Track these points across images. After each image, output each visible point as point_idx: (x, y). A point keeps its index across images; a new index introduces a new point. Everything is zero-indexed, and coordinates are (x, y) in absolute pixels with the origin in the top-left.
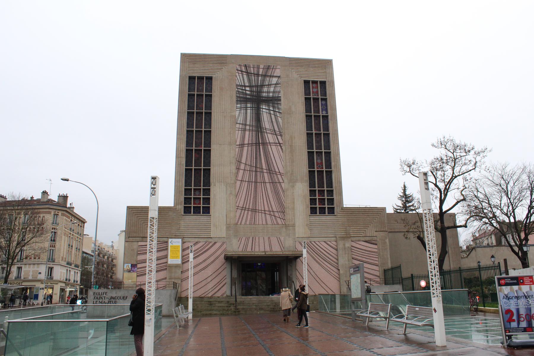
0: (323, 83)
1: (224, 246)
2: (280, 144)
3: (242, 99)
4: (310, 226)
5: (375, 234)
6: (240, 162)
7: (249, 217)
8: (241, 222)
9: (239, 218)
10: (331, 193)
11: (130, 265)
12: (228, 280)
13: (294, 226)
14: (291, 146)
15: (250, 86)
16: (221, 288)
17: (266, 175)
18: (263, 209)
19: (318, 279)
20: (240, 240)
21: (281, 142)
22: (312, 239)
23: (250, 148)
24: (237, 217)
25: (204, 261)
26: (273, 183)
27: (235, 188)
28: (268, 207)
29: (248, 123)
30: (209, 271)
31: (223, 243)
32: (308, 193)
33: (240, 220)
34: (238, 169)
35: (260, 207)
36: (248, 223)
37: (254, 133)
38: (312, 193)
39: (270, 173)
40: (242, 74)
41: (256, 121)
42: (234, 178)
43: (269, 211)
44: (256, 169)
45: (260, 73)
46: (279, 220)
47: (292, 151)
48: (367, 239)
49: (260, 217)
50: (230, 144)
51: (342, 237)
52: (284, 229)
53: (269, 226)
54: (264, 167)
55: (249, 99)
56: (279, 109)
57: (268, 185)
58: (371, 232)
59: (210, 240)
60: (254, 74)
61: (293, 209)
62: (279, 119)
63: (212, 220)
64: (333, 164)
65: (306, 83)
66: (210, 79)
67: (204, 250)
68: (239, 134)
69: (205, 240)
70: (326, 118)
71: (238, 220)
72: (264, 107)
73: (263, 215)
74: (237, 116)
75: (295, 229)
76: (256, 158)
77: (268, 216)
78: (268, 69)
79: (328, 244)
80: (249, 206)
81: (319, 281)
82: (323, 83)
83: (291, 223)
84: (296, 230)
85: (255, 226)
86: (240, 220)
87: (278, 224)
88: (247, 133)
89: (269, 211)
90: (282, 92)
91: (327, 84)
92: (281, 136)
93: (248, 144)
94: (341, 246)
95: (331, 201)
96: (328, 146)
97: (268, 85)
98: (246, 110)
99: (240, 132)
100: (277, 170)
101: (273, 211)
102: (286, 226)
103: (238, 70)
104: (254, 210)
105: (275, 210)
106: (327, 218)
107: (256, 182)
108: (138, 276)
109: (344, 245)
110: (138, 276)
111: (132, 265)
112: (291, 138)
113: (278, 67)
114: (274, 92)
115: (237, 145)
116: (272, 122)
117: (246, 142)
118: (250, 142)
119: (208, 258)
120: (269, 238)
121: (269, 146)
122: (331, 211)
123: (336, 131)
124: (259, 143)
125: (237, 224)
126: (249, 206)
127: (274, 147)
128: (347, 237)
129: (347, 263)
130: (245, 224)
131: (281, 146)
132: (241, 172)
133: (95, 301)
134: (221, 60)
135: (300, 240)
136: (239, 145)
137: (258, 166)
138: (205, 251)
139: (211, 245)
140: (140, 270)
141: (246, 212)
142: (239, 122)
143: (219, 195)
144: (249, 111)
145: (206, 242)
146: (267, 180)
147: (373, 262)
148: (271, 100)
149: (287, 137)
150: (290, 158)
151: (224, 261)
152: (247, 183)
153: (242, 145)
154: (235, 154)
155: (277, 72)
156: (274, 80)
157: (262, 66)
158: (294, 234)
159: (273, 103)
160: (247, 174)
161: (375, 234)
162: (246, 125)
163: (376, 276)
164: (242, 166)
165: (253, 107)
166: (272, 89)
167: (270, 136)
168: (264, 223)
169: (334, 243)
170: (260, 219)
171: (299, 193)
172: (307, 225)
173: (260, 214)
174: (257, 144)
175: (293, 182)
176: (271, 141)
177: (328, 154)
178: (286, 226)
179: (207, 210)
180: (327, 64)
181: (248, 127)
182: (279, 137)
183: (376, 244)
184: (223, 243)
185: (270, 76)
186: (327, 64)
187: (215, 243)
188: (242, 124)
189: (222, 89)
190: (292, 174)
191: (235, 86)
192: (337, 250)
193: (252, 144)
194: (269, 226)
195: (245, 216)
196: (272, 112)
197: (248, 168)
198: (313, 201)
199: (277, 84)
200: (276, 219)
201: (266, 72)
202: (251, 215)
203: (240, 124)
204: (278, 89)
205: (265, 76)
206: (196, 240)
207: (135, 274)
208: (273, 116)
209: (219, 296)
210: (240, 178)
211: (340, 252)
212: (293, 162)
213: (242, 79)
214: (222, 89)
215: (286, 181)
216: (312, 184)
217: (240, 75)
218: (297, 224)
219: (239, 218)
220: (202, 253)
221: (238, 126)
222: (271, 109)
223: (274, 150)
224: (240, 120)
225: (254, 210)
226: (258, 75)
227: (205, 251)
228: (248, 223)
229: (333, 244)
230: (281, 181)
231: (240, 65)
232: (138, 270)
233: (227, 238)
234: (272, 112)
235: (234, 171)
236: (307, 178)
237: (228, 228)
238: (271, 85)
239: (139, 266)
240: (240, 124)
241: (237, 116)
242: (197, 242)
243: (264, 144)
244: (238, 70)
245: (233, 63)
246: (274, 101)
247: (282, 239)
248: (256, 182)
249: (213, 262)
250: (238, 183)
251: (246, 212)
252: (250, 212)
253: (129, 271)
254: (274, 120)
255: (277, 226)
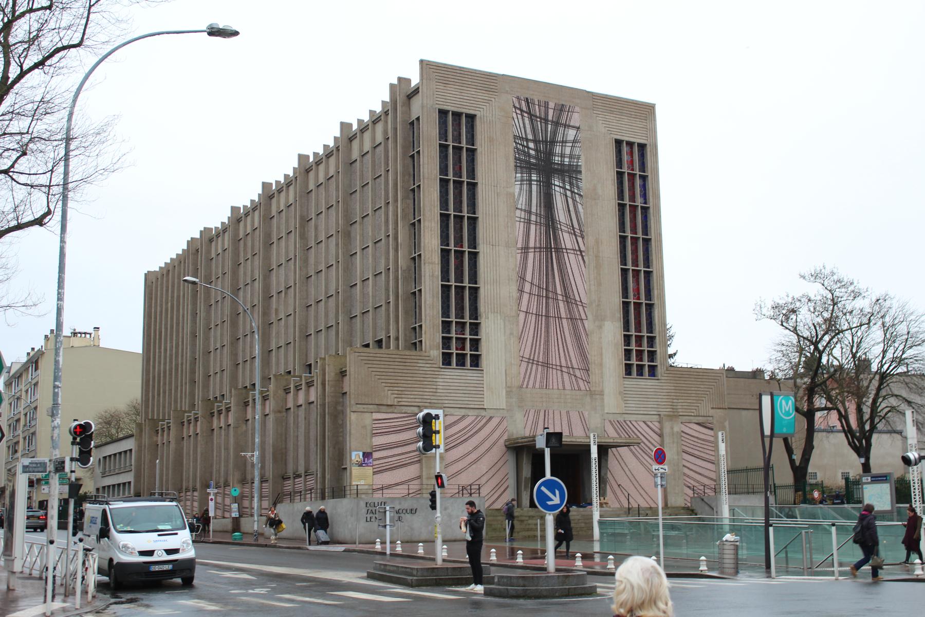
0: (642, 147)
1: (505, 423)
2: (581, 252)
3: (524, 165)
4: (624, 394)
5: (712, 412)
6: (523, 279)
7: (539, 376)
8: (528, 385)
9: (524, 378)
10: (651, 340)
11: (361, 454)
12: (512, 482)
13: (601, 393)
14: (597, 257)
15: (535, 141)
16: (501, 495)
17: (561, 304)
18: (558, 364)
19: (635, 482)
20: (527, 413)
21: (583, 248)
22: (633, 418)
23: (537, 254)
24: (522, 376)
25: (475, 448)
26: (572, 319)
27: (518, 325)
28: (566, 360)
29: (534, 210)
30: (483, 466)
31: (503, 419)
32: (621, 340)
33: (526, 380)
34: (521, 291)
35: (554, 360)
36: (537, 386)
37: (543, 228)
38: (627, 339)
39: (568, 302)
40: (522, 116)
41: (545, 207)
42: (515, 308)
43: (568, 367)
44: (546, 293)
45: (550, 118)
46: (581, 382)
47: (598, 267)
48: (701, 420)
49: (554, 375)
50: (507, 246)
51: (668, 416)
52: (588, 399)
53: (567, 392)
54: (559, 292)
55: (534, 165)
56: (578, 187)
57: (565, 322)
58: (705, 409)
59: (483, 413)
60: (540, 118)
61: (601, 365)
62: (580, 206)
63: (485, 379)
64: (655, 293)
65: (618, 143)
66: (471, 118)
67: (474, 430)
68: (520, 228)
69: (476, 412)
70: (645, 210)
71: (523, 381)
72: (557, 183)
73: (559, 372)
74: (516, 194)
75: (603, 399)
76: (547, 275)
77: (566, 376)
78: (561, 110)
79: (648, 426)
80: (538, 357)
81: (637, 486)
82: (642, 147)
83: (597, 389)
84: (606, 401)
85: (544, 391)
86: (526, 380)
87: (580, 389)
88: (533, 227)
89: (568, 367)
90: (582, 157)
91: (648, 149)
92: (583, 238)
93: (535, 248)
94: (667, 430)
95: (652, 355)
96: (647, 262)
97: (563, 142)
98: (530, 185)
99: (522, 224)
100: (577, 299)
101: (573, 368)
102: (591, 393)
103: (515, 107)
104: (546, 365)
105: (575, 366)
106: (646, 383)
107: (547, 316)
108: (375, 473)
109: (672, 428)
110: (375, 473)
111: (364, 453)
112: (597, 242)
113: (577, 109)
114: (571, 157)
115: (518, 249)
116: (569, 211)
117: (532, 244)
118: (538, 245)
119: (481, 443)
120: (568, 412)
121: (565, 254)
122: (653, 371)
123: (660, 235)
124: (551, 248)
125: (521, 387)
126: (538, 357)
127: (572, 257)
128: (674, 416)
129: (676, 457)
130: (534, 387)
131: (582, 256)
132: (526, 297)
133: (369, 516)
134: (489, 82)
135: (611, 417)
136: (522, 249)
137: (550, 289)
138: (476, 432)
139: (484, 421)
140: (377, 462)
141: (535, 366)
142: (519, 206)
143: (497, 336)
144: (534, 188)
145: (477, 416)
146: (563, 315)
147: (707, 457)
148: (568, 171)
149: (590, 240)
150: (596, 279)
151: (504, 448)
152: (534, 316)
153: (525, 249)
154: (516, 266)
155: (575, 120)
156: (571, 134)
157: (551, 105)
158: (603, 406)
159: (570, 177)
160: (535, 299)
161: (712, 412)
162: (530, 212)
163: (711, 479)
164: (527, 287)
165: (540, 181)
166: (568, 151)
167: (566, 235)
168: (561, 387)
169: (657, 424)
170: (555, 380)
171: (607, 339)
172: (620, 393)
173: (555, 371)
174: (548, 249)
175: (600, 319)
176: (569, 246)
177: (648, 274)
178: (591, 393)
179: (476, 361)
180: (646, 112)
181: (533, 218)
182: (580, 239)
183: (712, 429)
184: (503, 419)
185: (567, 126)
186: (646, 112)
187: (491, 418)
188: (525, 211)
189: (491, 140)
190: (598, 305)
191: (512, 139)
192: (661, 435)
193: (540, 248)
194: (567, 392)
195: (533, 373)
196: (569, 193)
197: (535, 290)
198: (628, 353)
199: (574, 141)
200: (577, 381)
201: (559, 118)
202: (542, 373)
203: (521, 210)
204: (577, 151)
205: (557, 124)
206: (463, 412)
207: (369, 470)
208: (570, 200)
209: (499, 507)
210: (524, 308)
211: (667, 440)
212: (599, 284)
213: (522, 126)
214: (491, 140)
215: (590, 317)
216: (626, 327)
217: (520, 116)
218: (606, 391)
219: (524, 378)
220: (472, 436)
221: (518, 212)
222: (568, 187)
223: (572, 260)
224: (522, 203)
225: (546, 365)
226: (546, 120)
227: (476, 432)
228: (537, 386)
229: (656, 426)
230: (583, 317)
231: (518, 98)
232: (375, 463)
233: (508, 411)
234: (569, 193)
235: (515, 294)
236: (619, 314)
237: (509, 393)
238: (566, 142)
239: (376, 455)
240: (521, 210)
241: (516, 194)
242: (464, 416)
243: (558, 250)
244: (515, 107)
245: (507, 92)
246: (571, 173)
247: (586, 414)
248: (547, 316)
249: (488, 450)
250: (522, 315)
251: (535, 366)
252: (540, 368)
253: (361, 465)
254: (572, 208)
255: (578, 392)
